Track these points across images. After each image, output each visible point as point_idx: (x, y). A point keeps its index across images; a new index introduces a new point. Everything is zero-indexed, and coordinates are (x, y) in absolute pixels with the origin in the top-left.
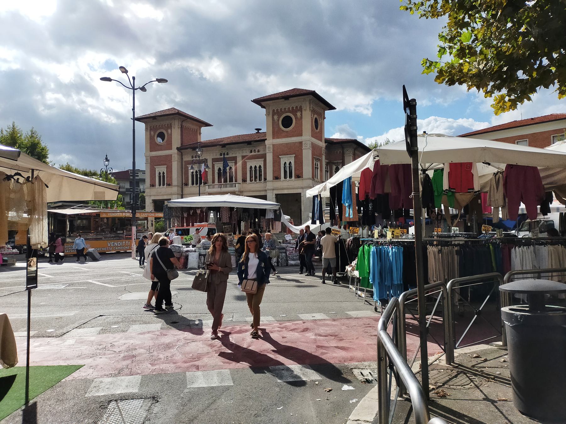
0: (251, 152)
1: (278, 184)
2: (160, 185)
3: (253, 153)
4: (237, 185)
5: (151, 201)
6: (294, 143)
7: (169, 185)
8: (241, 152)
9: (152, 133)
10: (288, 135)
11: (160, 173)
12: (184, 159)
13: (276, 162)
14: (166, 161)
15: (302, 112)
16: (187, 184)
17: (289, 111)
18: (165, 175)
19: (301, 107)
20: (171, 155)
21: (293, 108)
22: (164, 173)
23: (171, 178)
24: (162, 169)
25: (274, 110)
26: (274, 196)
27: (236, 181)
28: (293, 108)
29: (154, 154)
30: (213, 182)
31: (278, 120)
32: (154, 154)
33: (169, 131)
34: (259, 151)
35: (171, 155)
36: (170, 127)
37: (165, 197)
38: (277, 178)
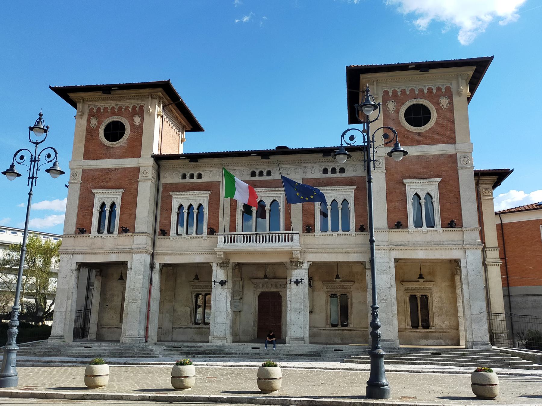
0: (325, 171)
1: (398, 236)
2: (99, 231)
3: (330, 175)
4: (296, 237)
5: (74, 267)
6: (437, 158)
7: (124, 230)
8: (300, 171)
9: (94, 122)
10: (420, 140)
11: (103, 205)
12: (163, 181)
13: (396, 193)
14: (127, 181)
15: (451, 97)
16: (164, 233)
17: (421, 95)
18: (118, 209)
19: (448, 89)
20: (137, 169)
21: (430, 90)
22: (113, 205)
23: (133, 216)
24: (113, 196)
25: (386, 93)
26: (393, 264)
27: (288, 227)
28: (430, 90)
29: (94, 164)
30: (233, 228)
31: (397, 111)
32: (94, 164)
33: (137, 120)
34: (342, 170)
35: (137, 169)
36: (141, 112)
37: (113, 258)
38: (398, 224)
